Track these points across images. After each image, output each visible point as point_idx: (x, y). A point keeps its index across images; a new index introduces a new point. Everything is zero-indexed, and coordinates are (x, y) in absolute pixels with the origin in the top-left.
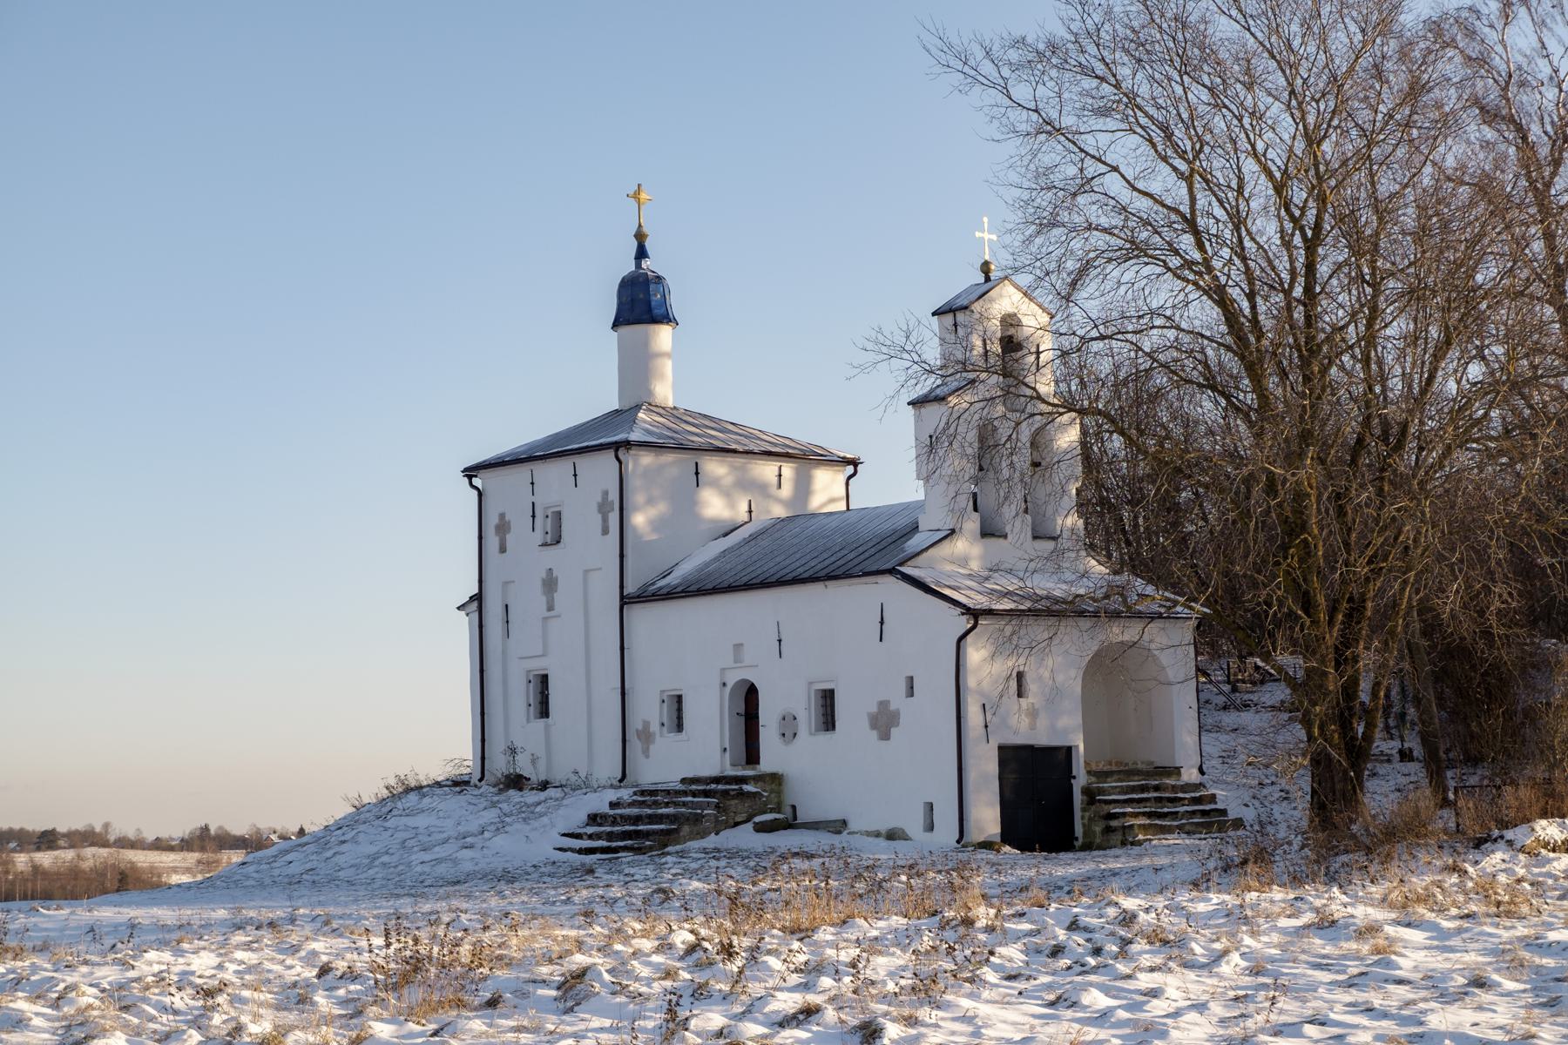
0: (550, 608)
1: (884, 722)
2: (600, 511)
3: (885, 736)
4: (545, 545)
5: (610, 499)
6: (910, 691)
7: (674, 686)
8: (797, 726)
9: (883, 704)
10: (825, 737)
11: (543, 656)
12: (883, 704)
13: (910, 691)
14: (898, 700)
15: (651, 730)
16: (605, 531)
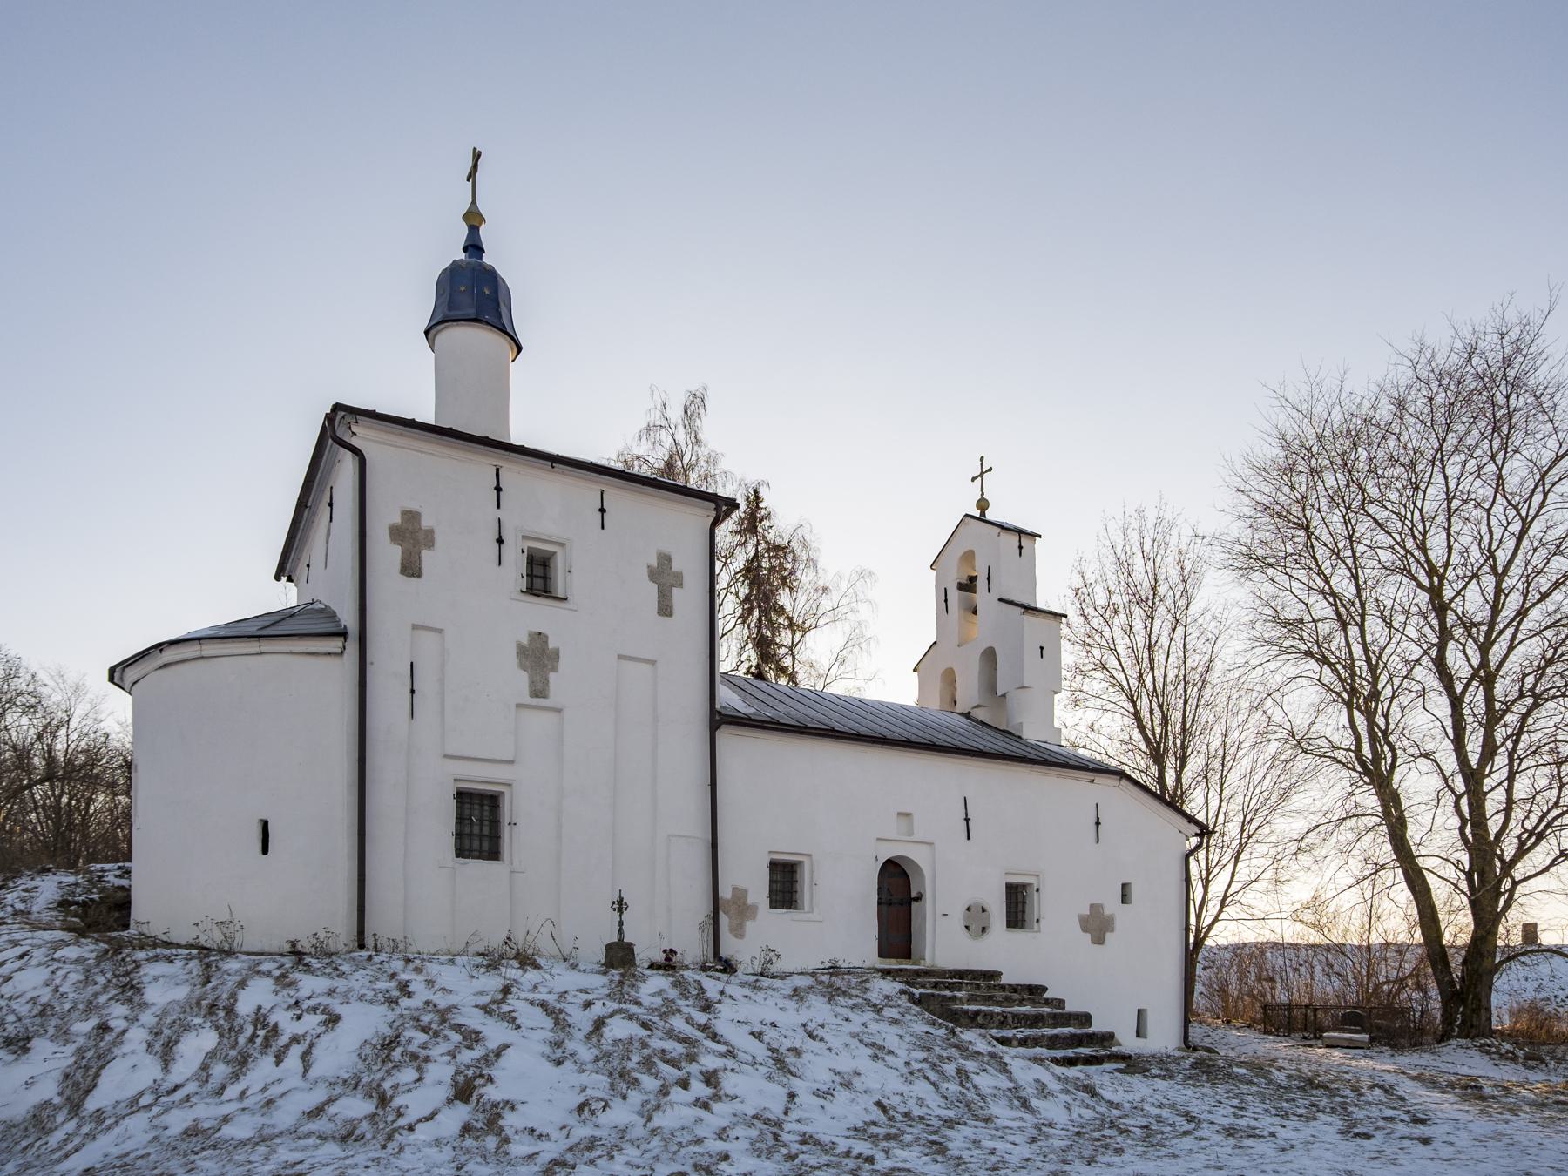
0: (539, 691)
1: (1097, 926)
2: (654, 575)
3: (1099, 940)
4: (522, 592)
5: (676, 567)
6: (1125, 897)
7: (786, 849)
8: (964, 920)
9: (1096, 909)
10: (1018, 935)
11: (512, 762)
12: (1096, 909)
13: (1125, 897)
14: (1112, 905)
15: (750, 901)
16: (665, 609)
